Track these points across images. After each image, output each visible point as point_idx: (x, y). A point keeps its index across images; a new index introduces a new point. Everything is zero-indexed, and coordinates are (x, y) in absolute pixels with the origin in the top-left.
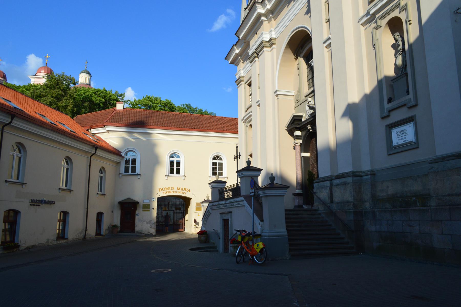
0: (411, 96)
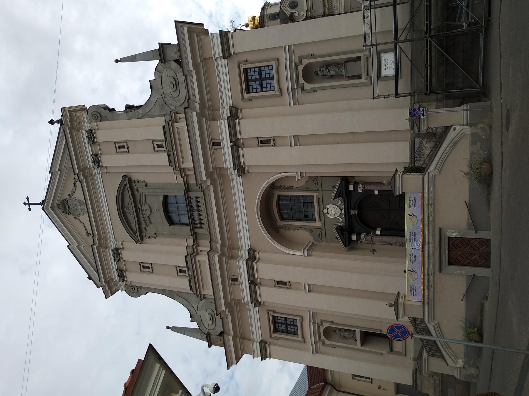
0: (361, 55)
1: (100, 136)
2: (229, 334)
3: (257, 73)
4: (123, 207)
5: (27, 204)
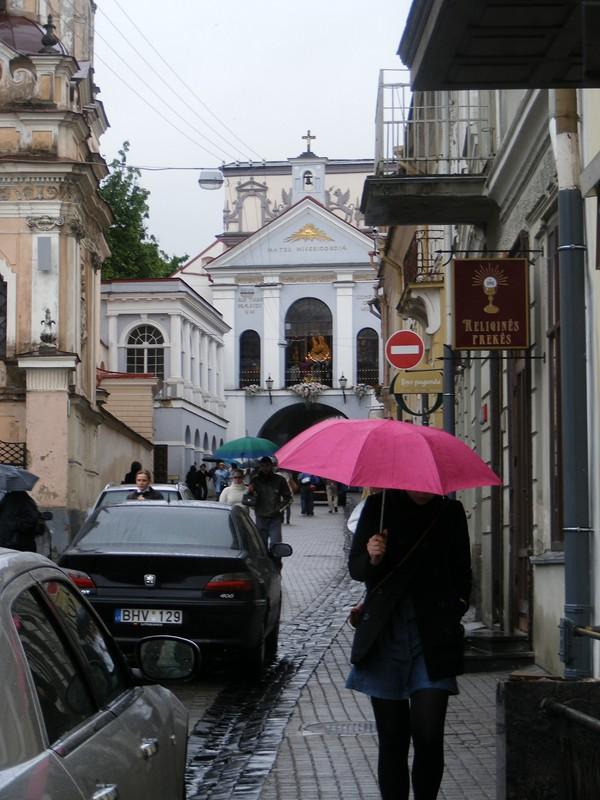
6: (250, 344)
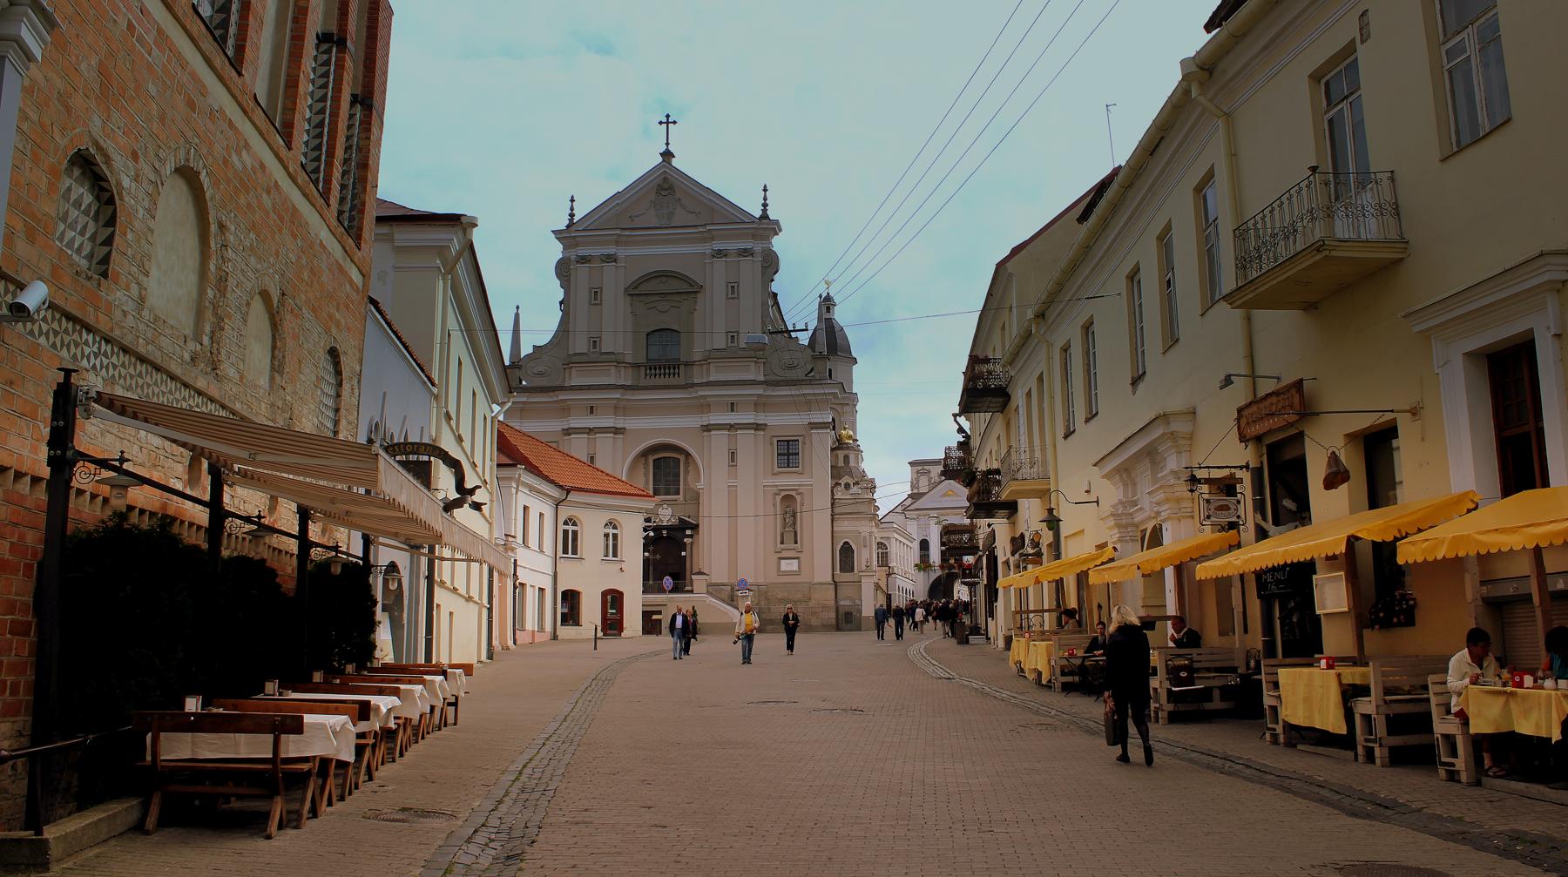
1: (746, 263)
2: (528, 398)
3: (794, 451)
4: (666, 276)
5: (668, 120)
6: (924, 545)
